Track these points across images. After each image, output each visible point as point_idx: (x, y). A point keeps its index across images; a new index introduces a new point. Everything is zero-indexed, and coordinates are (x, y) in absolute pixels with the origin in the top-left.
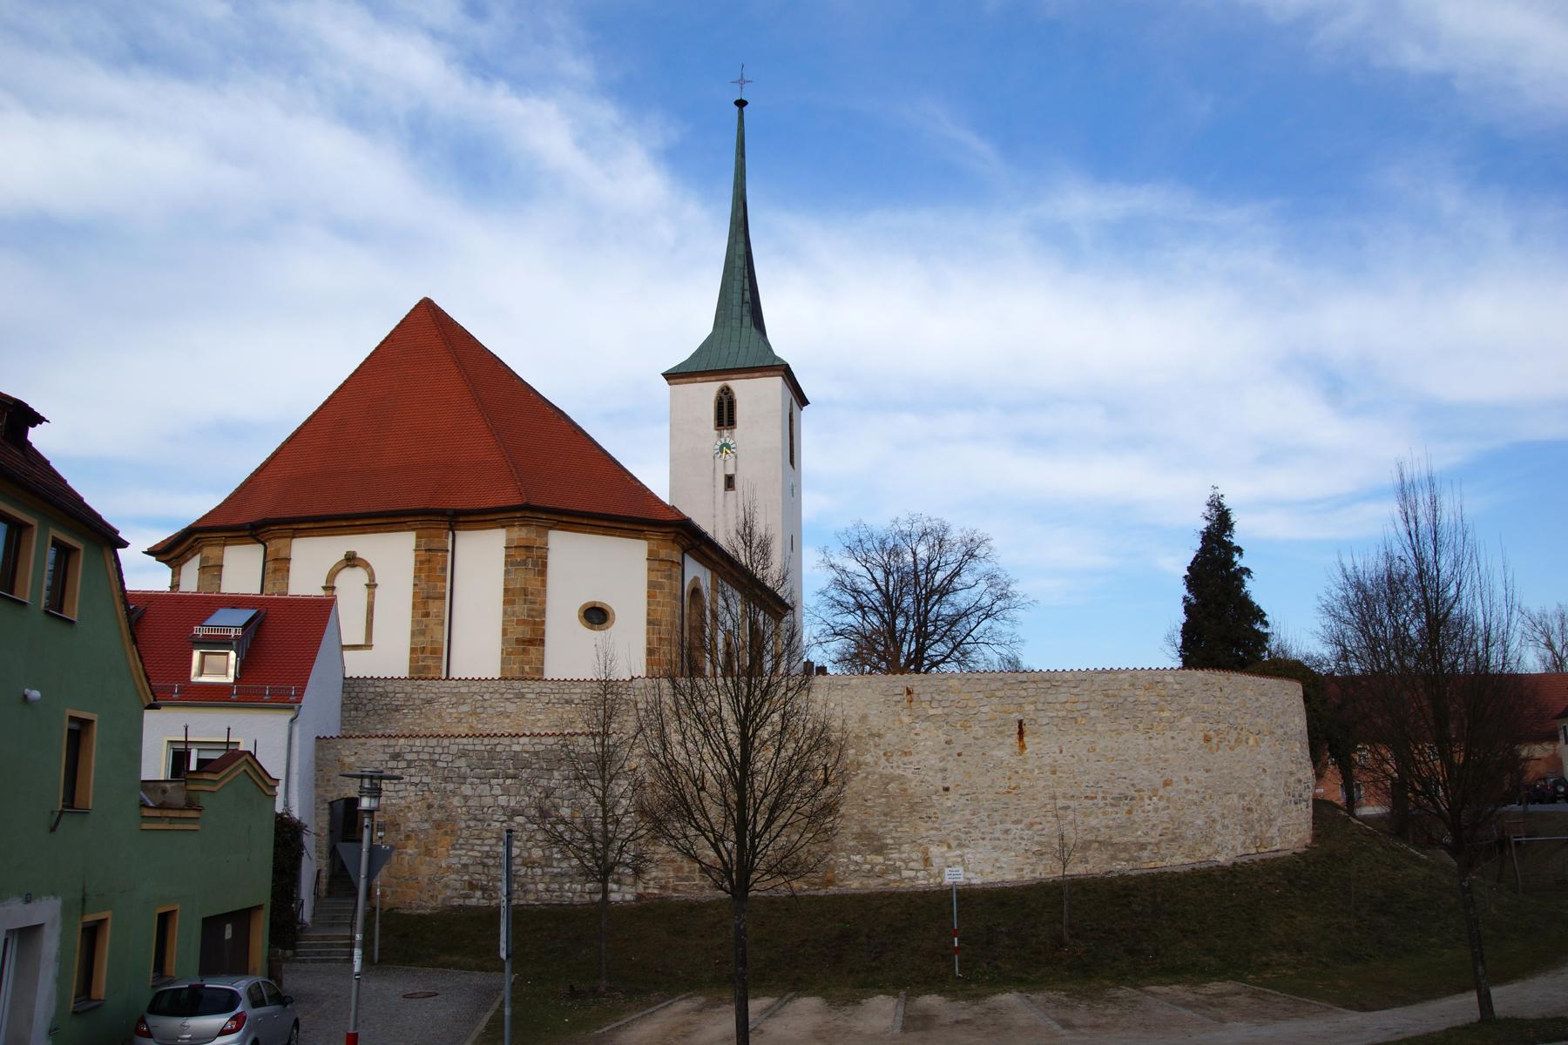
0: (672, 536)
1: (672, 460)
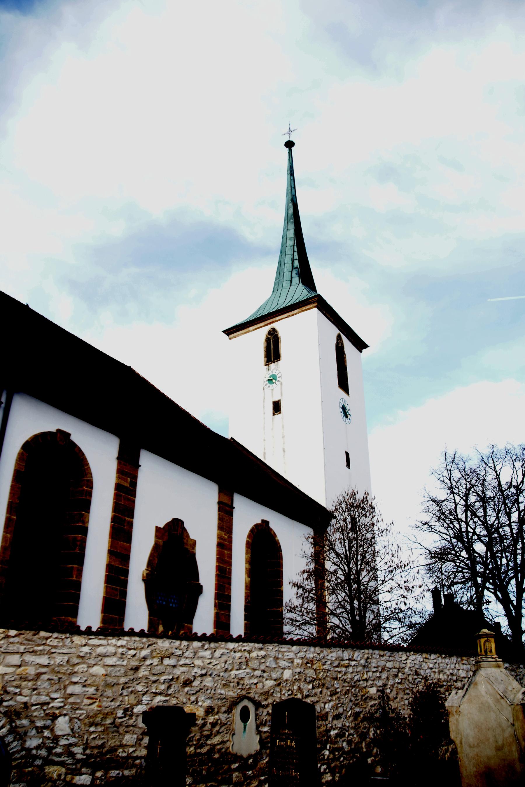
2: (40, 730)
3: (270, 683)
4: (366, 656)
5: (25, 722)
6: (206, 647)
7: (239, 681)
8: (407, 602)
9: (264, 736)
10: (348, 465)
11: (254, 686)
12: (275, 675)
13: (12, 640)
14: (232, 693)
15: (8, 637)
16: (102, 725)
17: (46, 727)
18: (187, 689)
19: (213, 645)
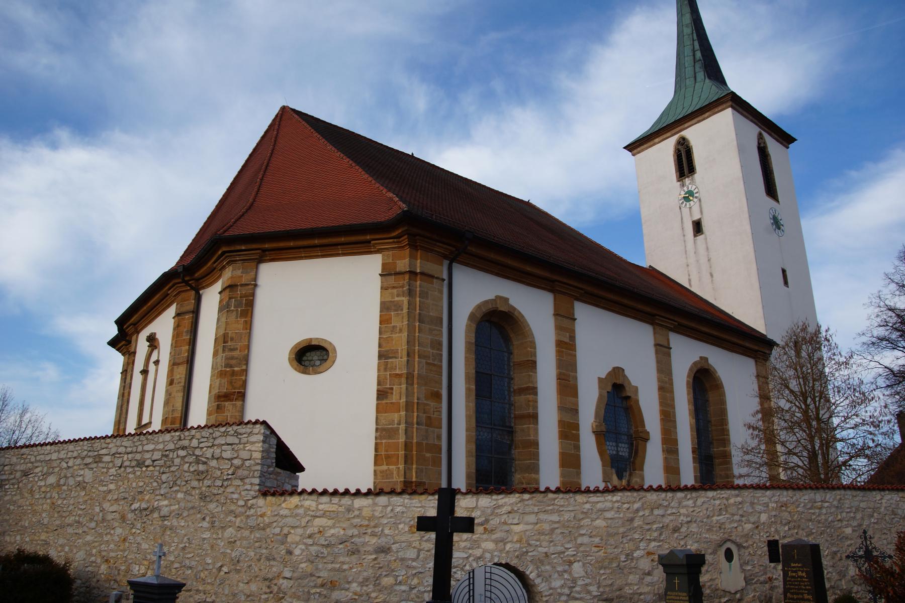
0: (405, 240)
2: (561, 574)
3: (748, 526)
4: (838, 497)
5: (548, 567)
6: (689, 497)
7: (721, 526)
8: (875, 438)
9: (748, 574)
10: (786, 283)
11: (734, 530)
12: (752, 519)
13: (526, 503)
14: (715, 537)
15: (522, 500)
16: (609, 568)
17: (565, 571)
18: (676, 535)
19: (694, 494)
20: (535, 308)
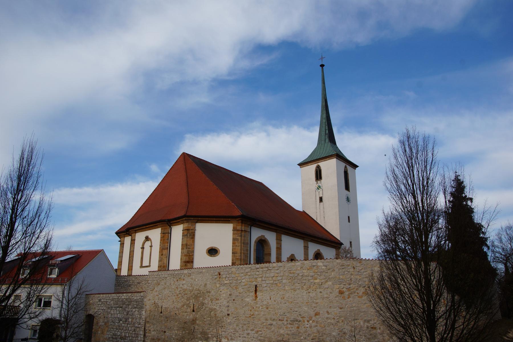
0: (240, 221)
1: (303, 194)
10: (349, 221)
20: (271, 237)
